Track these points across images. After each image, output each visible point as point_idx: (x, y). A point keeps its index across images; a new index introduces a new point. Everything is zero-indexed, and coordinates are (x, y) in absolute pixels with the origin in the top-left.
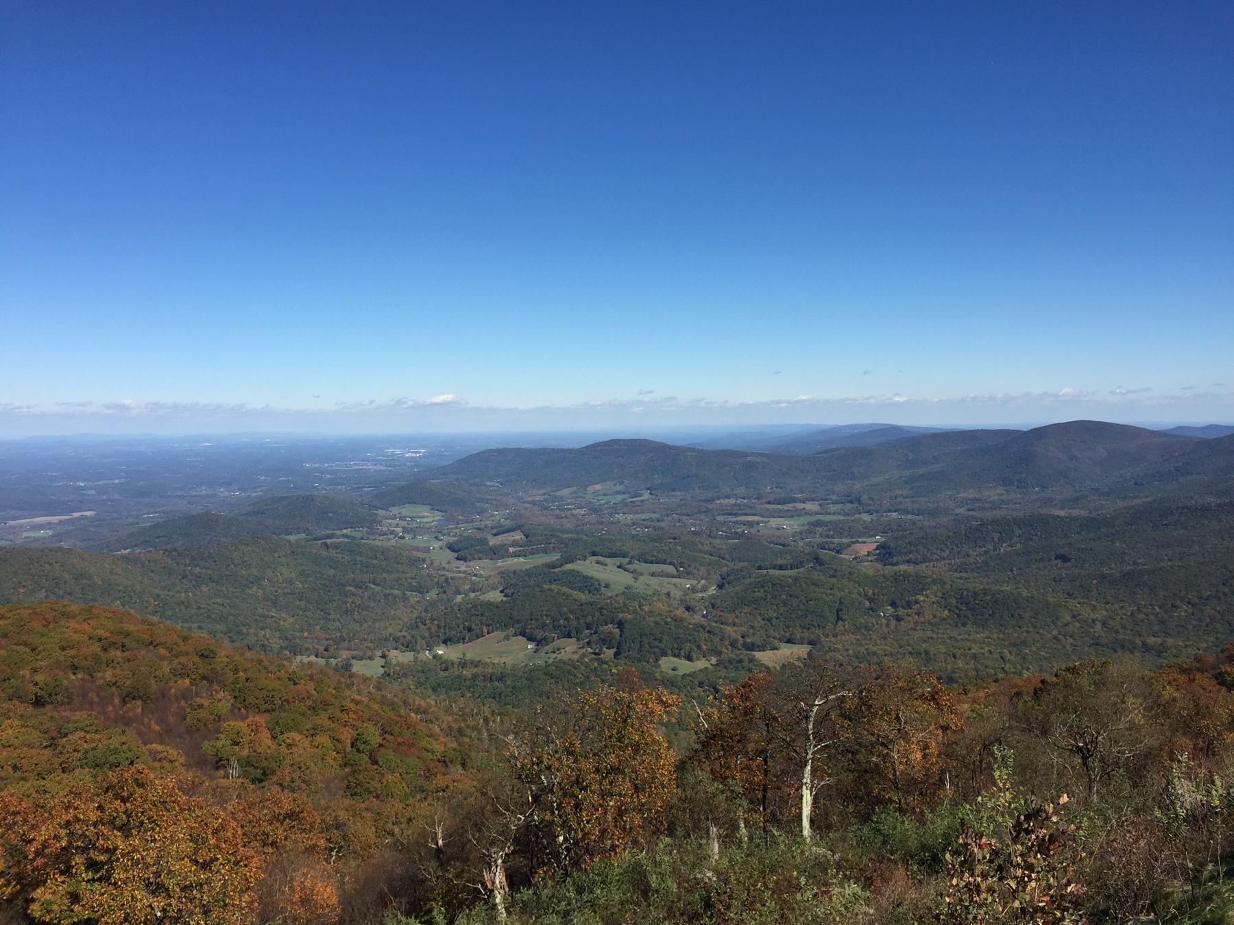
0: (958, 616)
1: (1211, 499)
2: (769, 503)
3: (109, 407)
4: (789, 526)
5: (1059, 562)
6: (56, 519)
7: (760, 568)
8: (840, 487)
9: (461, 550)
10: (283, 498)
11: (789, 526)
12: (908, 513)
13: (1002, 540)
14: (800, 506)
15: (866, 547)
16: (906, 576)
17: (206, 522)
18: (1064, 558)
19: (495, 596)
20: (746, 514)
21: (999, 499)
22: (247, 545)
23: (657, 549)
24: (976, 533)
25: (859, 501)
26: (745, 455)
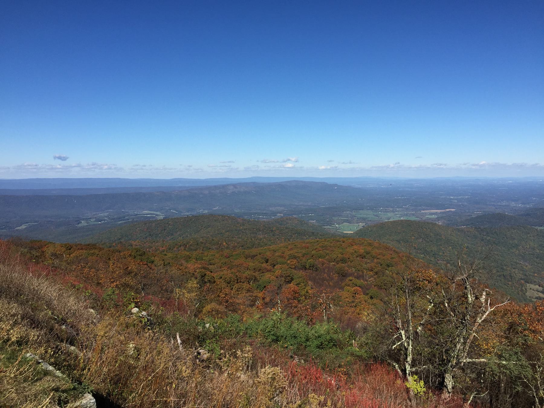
3: (474, 165)
6: (439, 211)
10: (541, 209)
17: (500, 217)
22: (514, 229)
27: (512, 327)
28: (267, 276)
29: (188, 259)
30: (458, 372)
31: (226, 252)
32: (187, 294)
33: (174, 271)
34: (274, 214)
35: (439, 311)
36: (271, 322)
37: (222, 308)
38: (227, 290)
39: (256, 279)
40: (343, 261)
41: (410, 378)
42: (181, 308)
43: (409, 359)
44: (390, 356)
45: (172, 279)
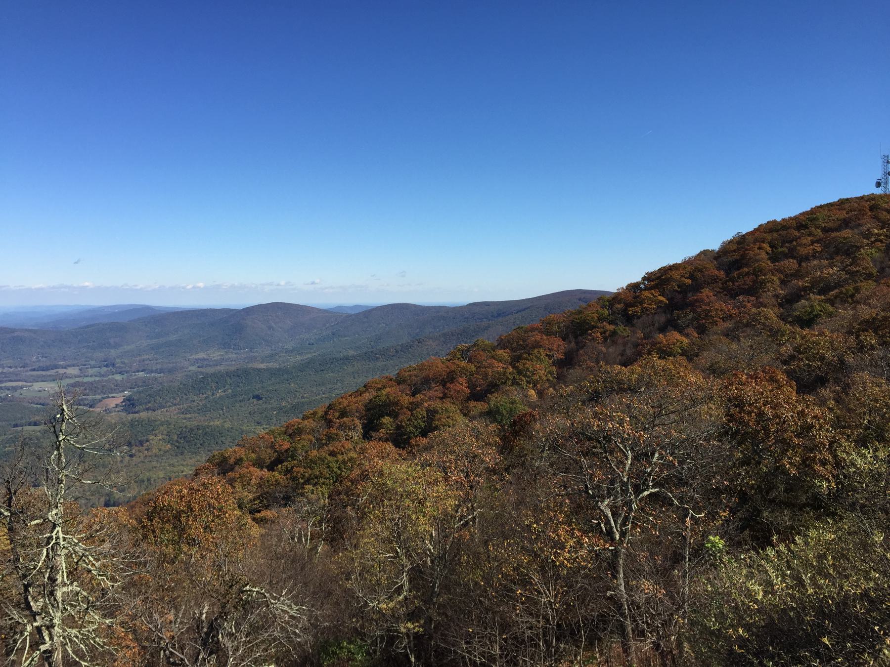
0: (178, 447)
1: (351, 353)
2: (34, 370)
4: (50, 387)
5: (255, 400)
7: (16, 426)
8: (100, 355)
11: (50, 387)
12: (152, 372)
13: (217, 388)
14: (61, 371)
15: (115, 400)
16: (140, 422)
18: (258, 398)
20: (11, 381)
24: (200, 384)
25: (113, 365)
26: (13, 331)
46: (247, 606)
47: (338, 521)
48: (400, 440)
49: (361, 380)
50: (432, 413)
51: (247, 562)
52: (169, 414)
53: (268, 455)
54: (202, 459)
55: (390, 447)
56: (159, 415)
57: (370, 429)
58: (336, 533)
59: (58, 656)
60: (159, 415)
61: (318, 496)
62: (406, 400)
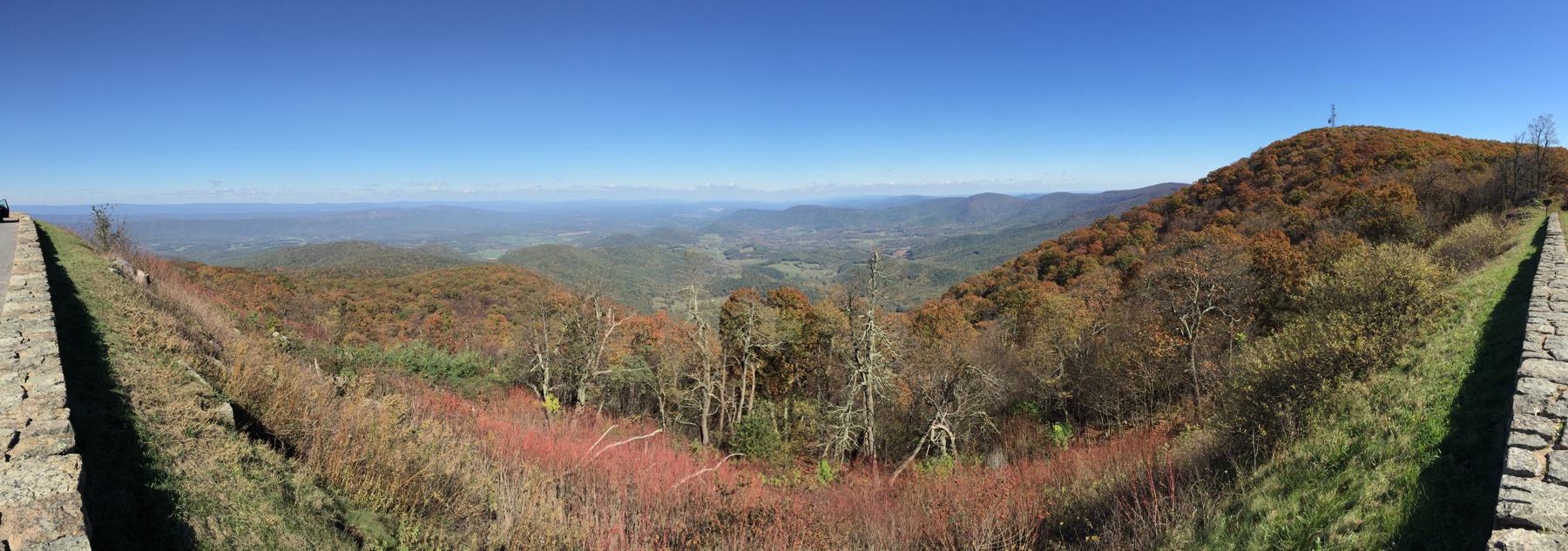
9: (728, 255)
11: (870, 242)
15: (902, 252)
19: (738, 276)
21: (957, 228)
23: (815, 257)
24: (945, 244)
27: (638, 336)
28: (411, 305)
29: (330, 286)
30: (590, 385)
31: (369, 280)
32: (329, 321)
33: (315, 298)
34: (419, 241)
35: (573, 332)
36: (411, 353)
37: (363, 337)
38: (369, 319)
39: (399, 309)
40: (487, 288)
41: (547, 398)
42: (321, 335)
43: (546, 380)
44: (530, 380)
45: (312, 306)
46: (969, 377)
47: (1022, 329)
48: (1061, 280)
49: (1037, 243)
50: (1080, 263)
51: (969, 352)
52: (929, 261)
53: (982, 288)
54: (946, 289)
55: (1054, 284)
56: (923, 262)
57: (1042, 273)
58: (1021, 338)
59: (870, 390)
60: (923, 262)
61: (1011, 314)
62: (1065, 254)
